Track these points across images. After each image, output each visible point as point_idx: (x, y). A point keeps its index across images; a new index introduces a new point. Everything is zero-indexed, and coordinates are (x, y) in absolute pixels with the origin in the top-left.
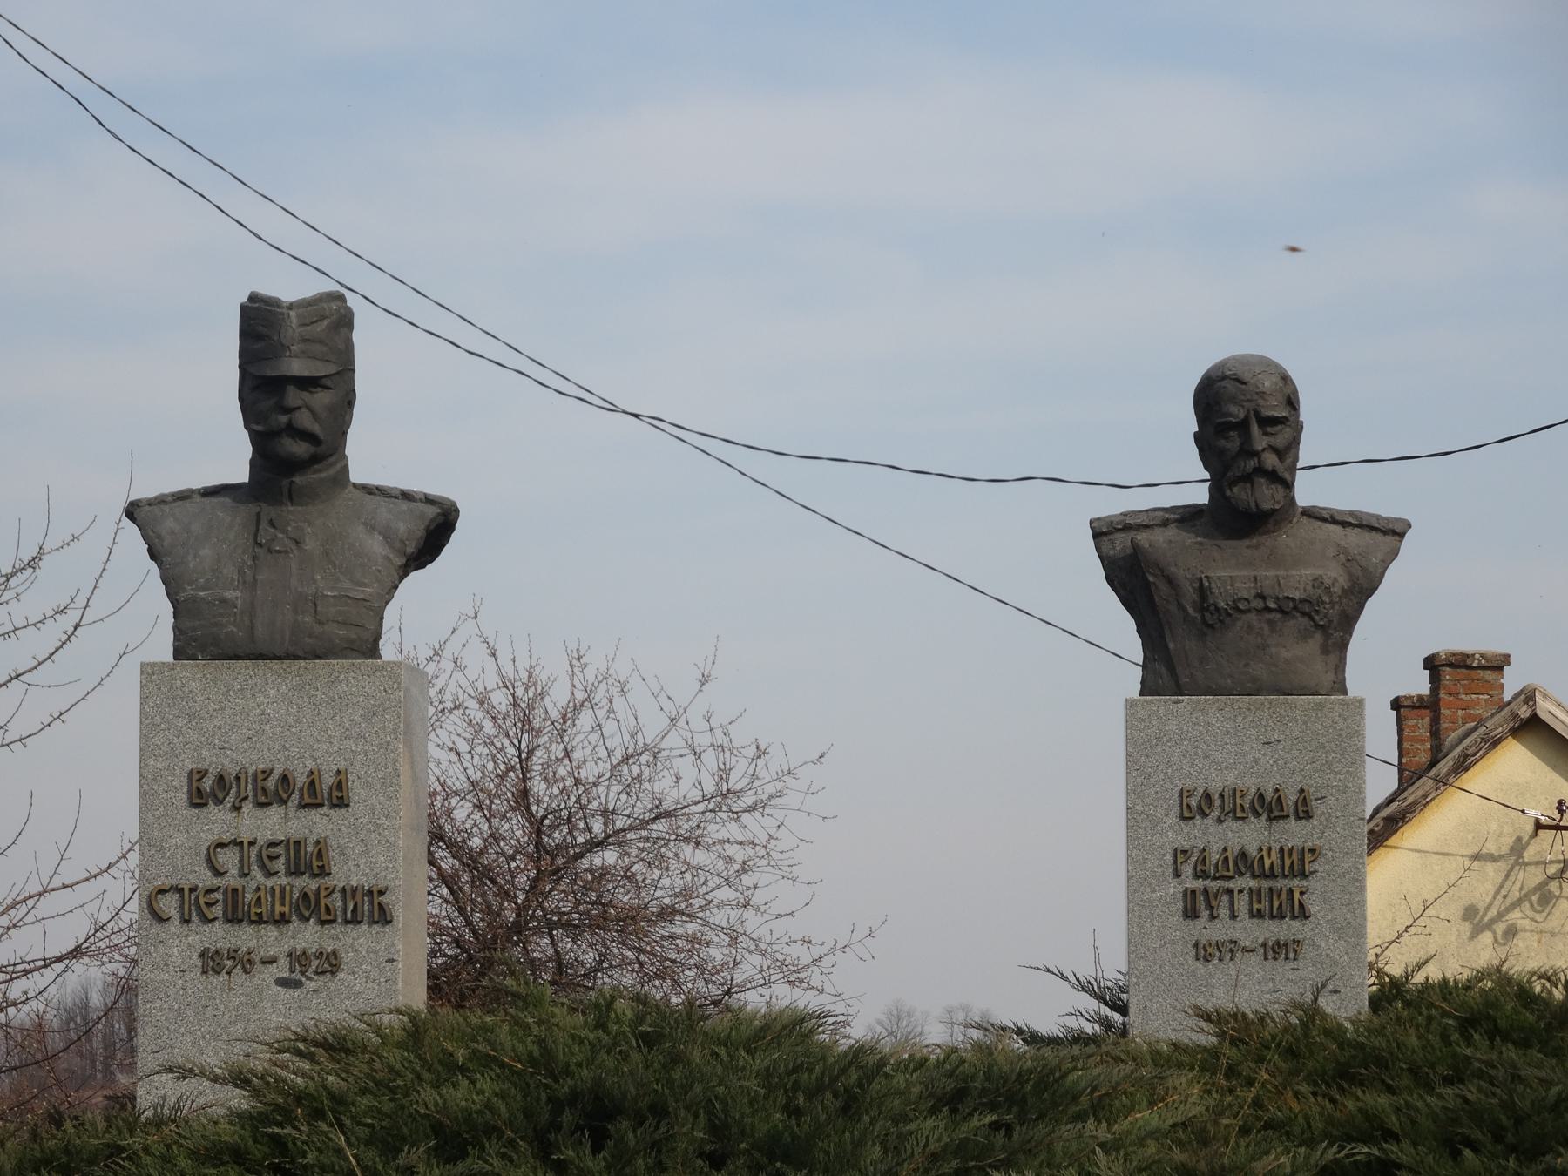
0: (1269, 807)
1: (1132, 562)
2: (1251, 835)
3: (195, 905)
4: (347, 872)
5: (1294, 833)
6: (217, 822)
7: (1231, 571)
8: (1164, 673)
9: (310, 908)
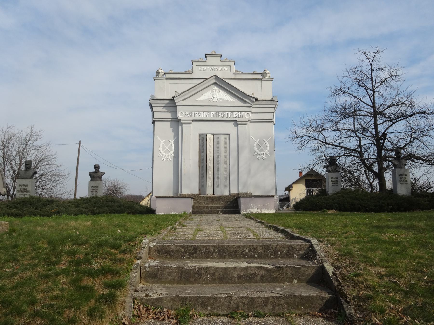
0: (96, 187)
1: (90, 174)
2: (95, 188)
3: (19, 191)
4: (27, 190)
5: (97, 188)
6: (21, 187)
7: (95, 175)
8: (91, 180)
9: (25, 192)
